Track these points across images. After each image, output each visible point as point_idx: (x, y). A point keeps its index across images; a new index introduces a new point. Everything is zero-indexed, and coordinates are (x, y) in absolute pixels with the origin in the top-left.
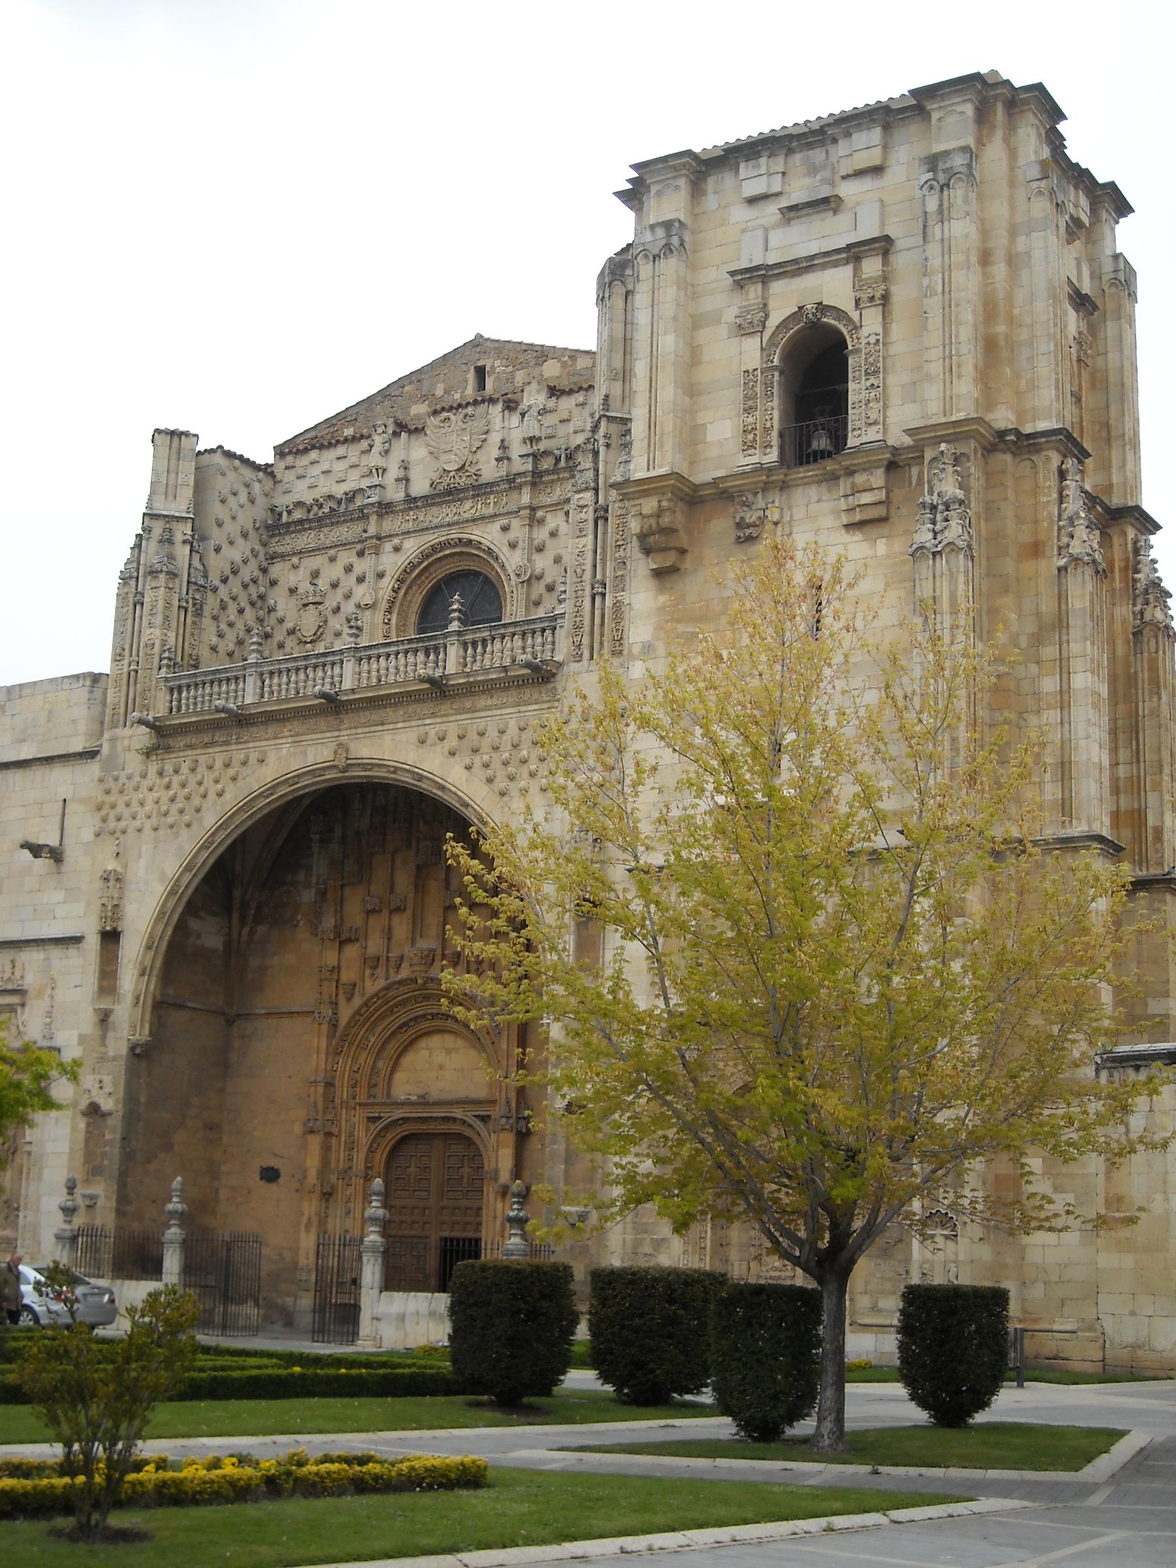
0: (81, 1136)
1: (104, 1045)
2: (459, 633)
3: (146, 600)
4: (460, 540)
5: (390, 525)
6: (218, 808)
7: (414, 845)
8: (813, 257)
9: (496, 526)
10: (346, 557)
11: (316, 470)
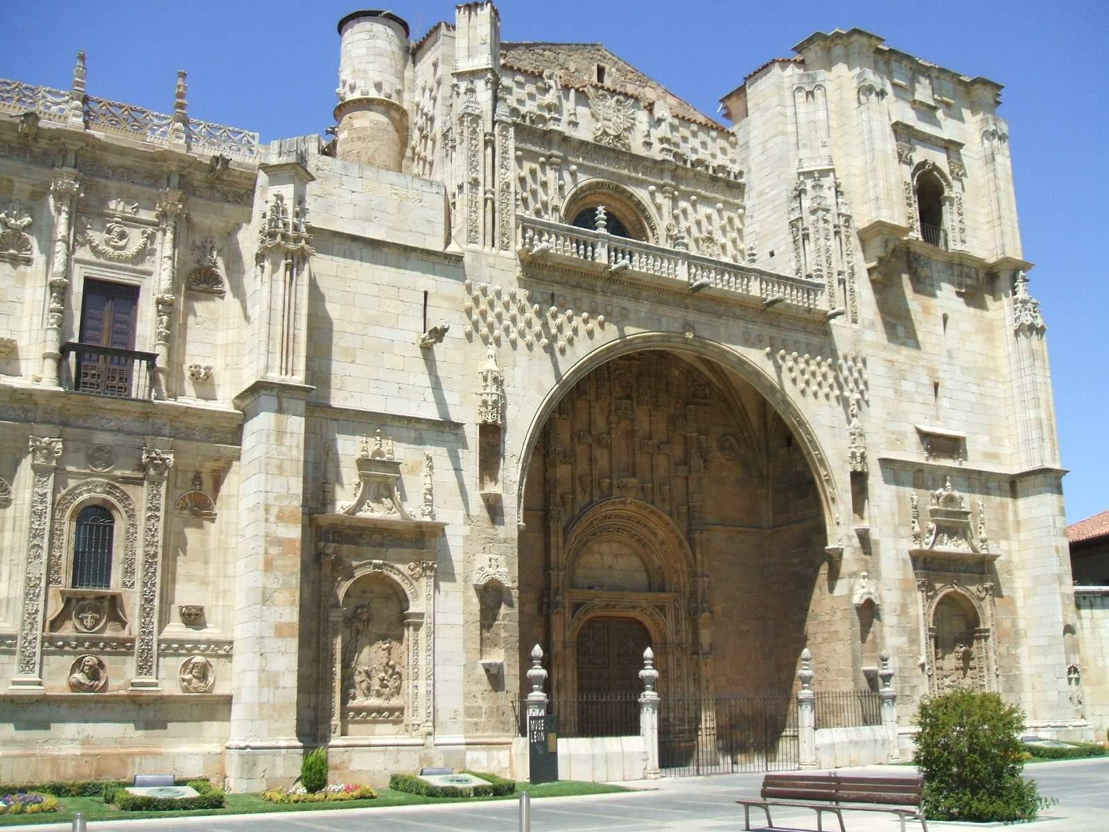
4: (617, 187)
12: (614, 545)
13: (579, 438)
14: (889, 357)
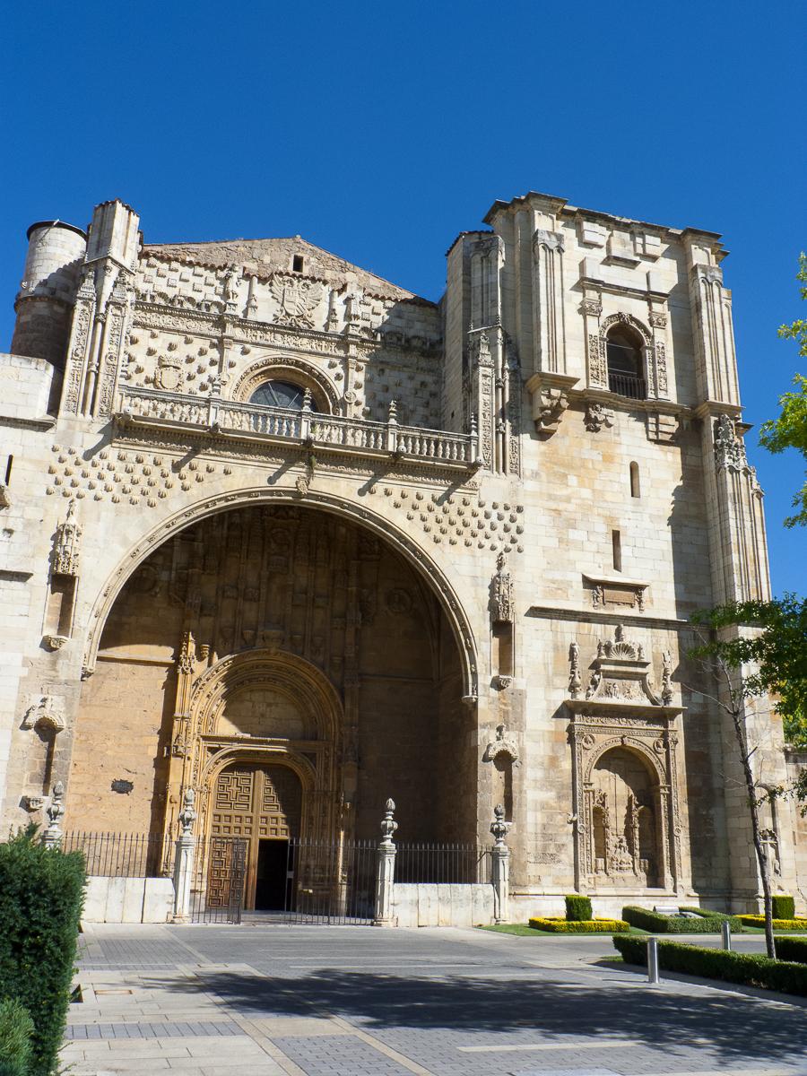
1: (54, 670)
5: (239, 333)
6: (185, 498)
7: (266, 556)
8: (627, 289)
9: (326, 361)
10: (199, 343)
11: (176, 276)
12: (268, 694)
13: (224, 592)
14: (554, 506)
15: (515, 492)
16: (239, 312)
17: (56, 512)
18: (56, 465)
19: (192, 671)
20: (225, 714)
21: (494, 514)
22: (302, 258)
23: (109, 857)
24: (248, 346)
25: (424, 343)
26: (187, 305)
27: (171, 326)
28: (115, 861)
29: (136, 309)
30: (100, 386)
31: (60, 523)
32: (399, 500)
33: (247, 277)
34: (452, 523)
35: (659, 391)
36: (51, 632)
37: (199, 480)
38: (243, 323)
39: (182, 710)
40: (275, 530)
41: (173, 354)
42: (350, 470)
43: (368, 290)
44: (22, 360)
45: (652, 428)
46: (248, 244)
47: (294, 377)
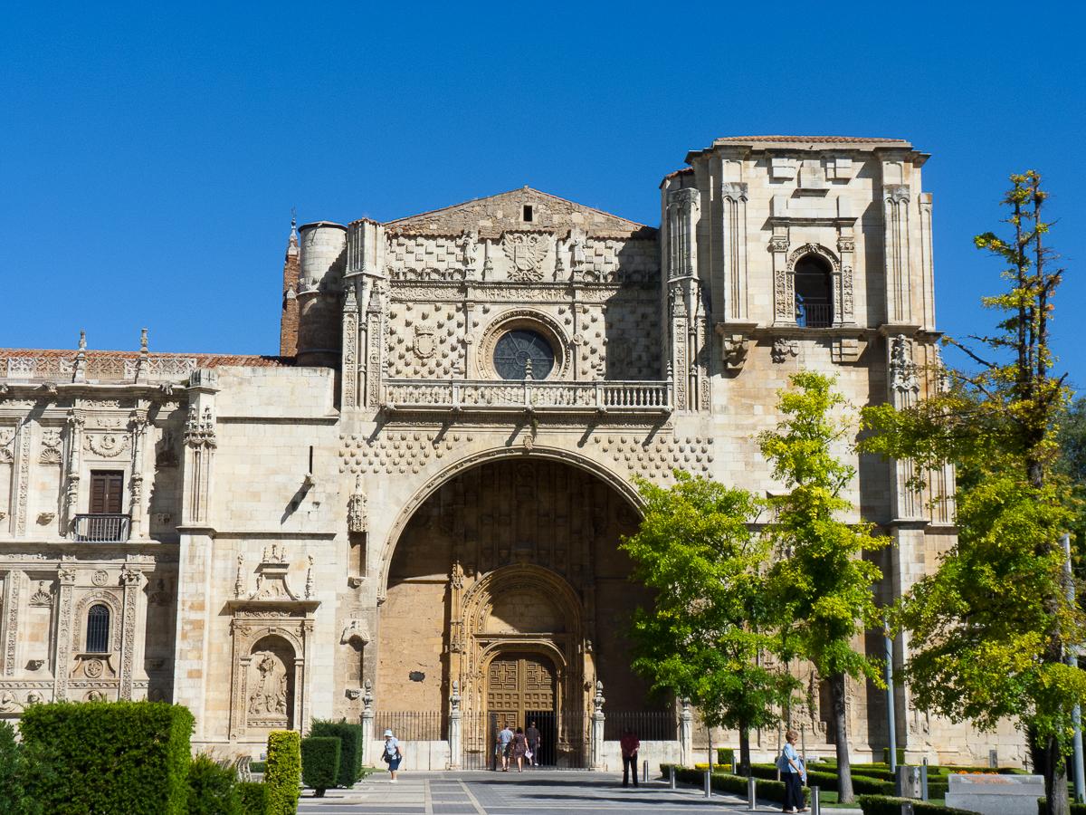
0: (344, 656)
2: (604, 383)
3: (370, 329)
9: (556, 308)
11: (421, 250)
14: (741, 434)
15: (706, 427)
16: (478, 277)
17: (348, 486)
18: (344, 450)
19: (462, 587)
20: (493, 614)
21: (687, 448)
22: (531, 207)
23: (413, 728)
24: (487, 306)
25: (643, 277)
26: (435, 276)
27: (422, 298)
28: (417, 731)
29: (392, 287)
30: (368, 382)
31: (352, 494)
32: (607, 445)
33: (482, 241)
34: (651, 460)
35: (844, 314)
36: (355, 574)
37: (449, 449)
38: (481, 285)
39: (456, 617)
40: (519, 466)
41: (427, 323)
42: (565, 426)
43: (590, 234)
44: (311, 371)
45: (836, 351)
46: (482, 203)
47: (531, 324)
